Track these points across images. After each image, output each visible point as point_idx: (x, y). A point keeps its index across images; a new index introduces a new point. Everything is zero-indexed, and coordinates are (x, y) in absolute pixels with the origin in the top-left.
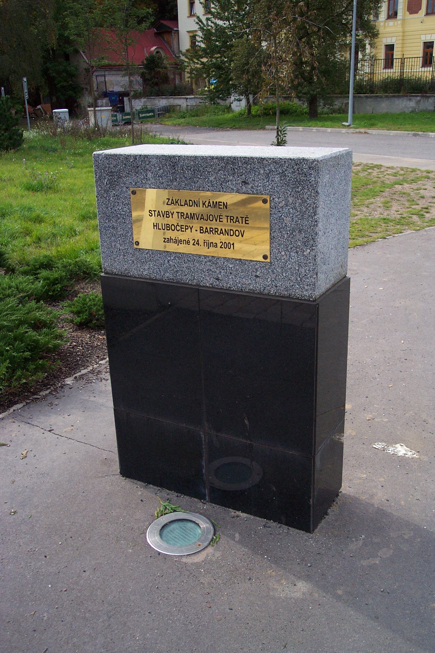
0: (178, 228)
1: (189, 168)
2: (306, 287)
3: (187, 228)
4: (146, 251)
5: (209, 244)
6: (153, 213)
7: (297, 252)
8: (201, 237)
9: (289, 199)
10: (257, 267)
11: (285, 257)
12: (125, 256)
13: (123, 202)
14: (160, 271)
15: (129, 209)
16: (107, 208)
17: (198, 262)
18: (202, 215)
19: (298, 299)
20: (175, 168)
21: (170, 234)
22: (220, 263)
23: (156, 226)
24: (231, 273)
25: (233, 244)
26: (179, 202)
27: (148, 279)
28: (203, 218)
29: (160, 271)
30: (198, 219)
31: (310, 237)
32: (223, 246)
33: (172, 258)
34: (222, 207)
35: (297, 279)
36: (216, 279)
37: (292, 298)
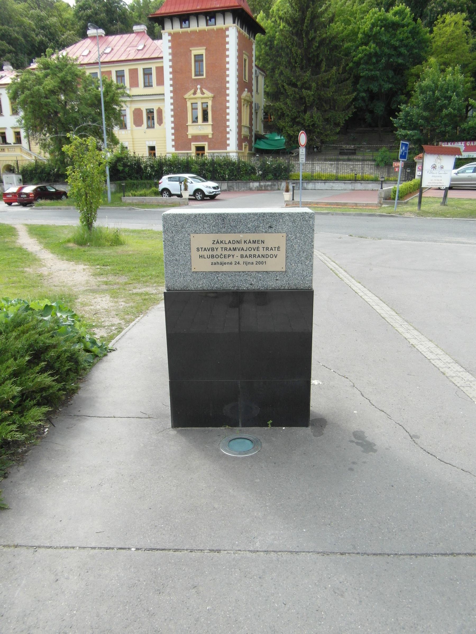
0: (221, 256)
1: (234, 220)
2: (307, 282)
3: (229, 256)
4: (201, 273)
5: (246, 263)
6: (200, 249)
7: (302, 263)
8: (241, 261)
9: (297, 235)
10: (277, 274)
11: (294, 267)
12: (184, 277)
13: (185, 244)
14: (211, 284)
15: (189, 248)
16: (172, 248)
17: (238, 275)
18: (242, 248)
19: (302, 289)
20: (224, 221)
21: (215, 260)
22: (253, 274)
23: (202, 257)
24: (260, 280)
25: (265, 262)
26: (223, 242)
27: (202, 290)
28: (243, 250)
29: (211, 284)
30: (239, 250)
31: (309, 254)
32: (258, 263)
33: (220, 275)
34: (260, 243)
35: (301, 278)
36: (250, 284)
37: (298, 289)
